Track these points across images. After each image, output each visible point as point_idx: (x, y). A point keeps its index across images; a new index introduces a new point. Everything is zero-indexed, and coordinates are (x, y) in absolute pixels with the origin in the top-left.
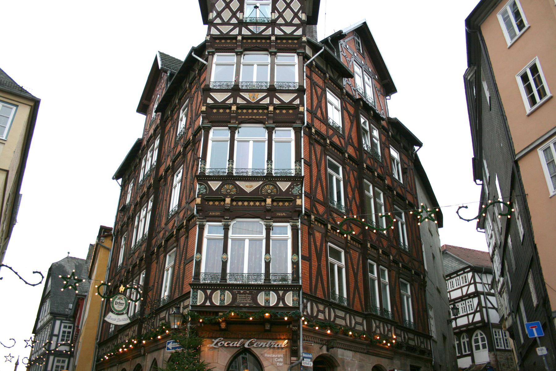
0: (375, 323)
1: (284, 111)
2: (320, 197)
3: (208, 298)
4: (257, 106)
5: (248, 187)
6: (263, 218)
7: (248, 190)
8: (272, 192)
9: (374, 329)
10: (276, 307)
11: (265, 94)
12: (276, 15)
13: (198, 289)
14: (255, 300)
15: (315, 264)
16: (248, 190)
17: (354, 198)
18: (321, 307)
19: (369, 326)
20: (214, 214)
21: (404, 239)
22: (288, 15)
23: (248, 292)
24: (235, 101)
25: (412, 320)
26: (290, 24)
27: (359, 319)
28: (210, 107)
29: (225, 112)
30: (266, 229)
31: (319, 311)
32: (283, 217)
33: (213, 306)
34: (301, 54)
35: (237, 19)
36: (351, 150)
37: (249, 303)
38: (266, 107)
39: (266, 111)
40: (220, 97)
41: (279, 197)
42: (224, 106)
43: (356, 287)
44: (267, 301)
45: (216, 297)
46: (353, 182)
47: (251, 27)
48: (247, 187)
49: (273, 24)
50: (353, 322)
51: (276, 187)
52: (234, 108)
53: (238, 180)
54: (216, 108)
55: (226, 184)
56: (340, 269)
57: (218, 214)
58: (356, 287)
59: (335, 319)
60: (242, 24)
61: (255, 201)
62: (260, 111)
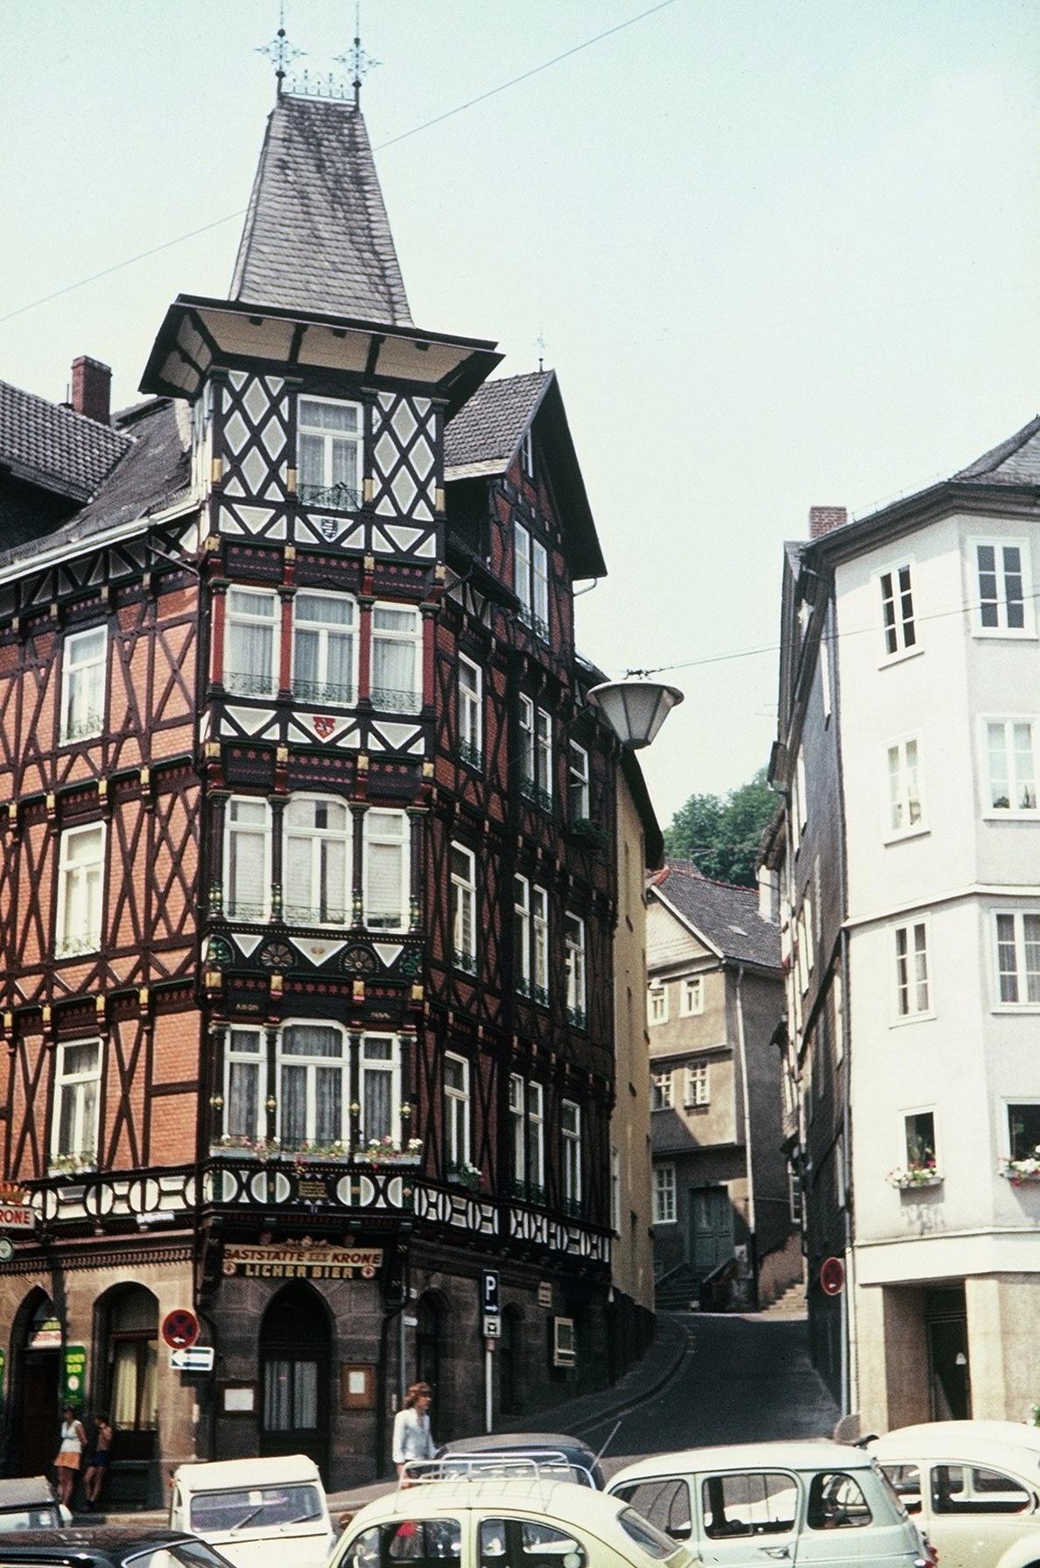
0: (516, 1217)
1: (389, 769)
2: (438, 953)
3: (244, 1187)
4: (332, 751)
5: (318, 954)
6: (347, 1024)
7: (318, 961)
8: (364, 967)
9: (512, 1232)
10: (371, 1208)
11: (353, 720)
12: (377, 486)
13: (221, 1169)
14: (332, 1192)
15: (425, 1105)
16: (318, 961)
17: (492, 927)
18: (433, 1197)
19: (504, 1223)
20: (244, 1007)
21: (576, 999)
22: (405, 490)
23: (319, 1176)
24: (284, 732)
25: (579, 1198)
26: (404, 520)
27: (489, 1211)
28: (227, 744)
29: (259, 759)
30: (351, 1047)
31: (431, 1205)
32: (384, 1021)
33: (254, 1203)
34: (430, 614)
35: (283, 487)
36: (495, 808)
37: (322, 1199)
38: (352, 755)
39: (349, 765)
40: (252, 722)
41: (377, 976)
42: (255, 745)
43: (486, 1141)
44: (356, 1197)
45: (259, 1185)
46: (492, 885)
47: (314, 519)
48: (314, 951)
49: (366, 516)
50: (478, 1219)
51: (374, 956)
52: (282, 753)
53: (293, 936)
54: (239, 748)
55: (271, 943)
56: (460, 1104)
57: (253, 1007)
58: (486, 1141)
59: (451, 1217)
60: (292, 507)
61: (328, 984)
62: (338, 764)
